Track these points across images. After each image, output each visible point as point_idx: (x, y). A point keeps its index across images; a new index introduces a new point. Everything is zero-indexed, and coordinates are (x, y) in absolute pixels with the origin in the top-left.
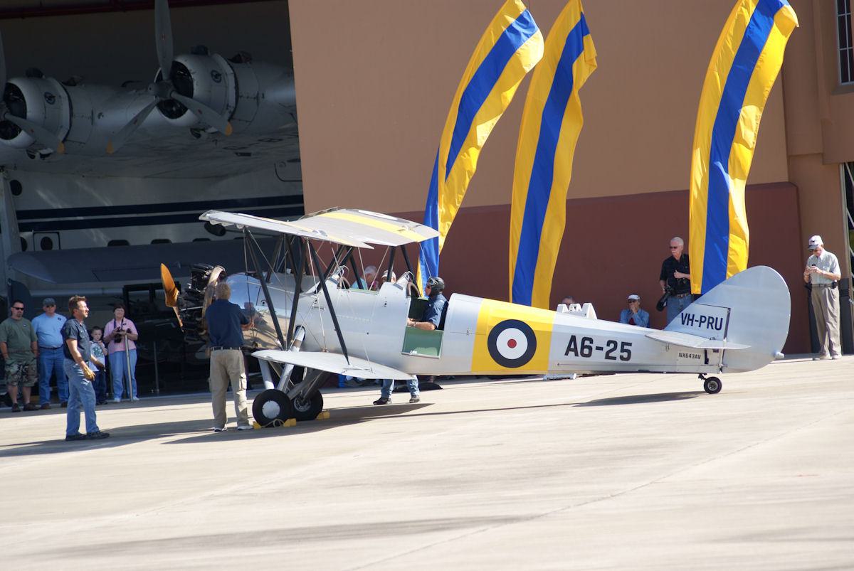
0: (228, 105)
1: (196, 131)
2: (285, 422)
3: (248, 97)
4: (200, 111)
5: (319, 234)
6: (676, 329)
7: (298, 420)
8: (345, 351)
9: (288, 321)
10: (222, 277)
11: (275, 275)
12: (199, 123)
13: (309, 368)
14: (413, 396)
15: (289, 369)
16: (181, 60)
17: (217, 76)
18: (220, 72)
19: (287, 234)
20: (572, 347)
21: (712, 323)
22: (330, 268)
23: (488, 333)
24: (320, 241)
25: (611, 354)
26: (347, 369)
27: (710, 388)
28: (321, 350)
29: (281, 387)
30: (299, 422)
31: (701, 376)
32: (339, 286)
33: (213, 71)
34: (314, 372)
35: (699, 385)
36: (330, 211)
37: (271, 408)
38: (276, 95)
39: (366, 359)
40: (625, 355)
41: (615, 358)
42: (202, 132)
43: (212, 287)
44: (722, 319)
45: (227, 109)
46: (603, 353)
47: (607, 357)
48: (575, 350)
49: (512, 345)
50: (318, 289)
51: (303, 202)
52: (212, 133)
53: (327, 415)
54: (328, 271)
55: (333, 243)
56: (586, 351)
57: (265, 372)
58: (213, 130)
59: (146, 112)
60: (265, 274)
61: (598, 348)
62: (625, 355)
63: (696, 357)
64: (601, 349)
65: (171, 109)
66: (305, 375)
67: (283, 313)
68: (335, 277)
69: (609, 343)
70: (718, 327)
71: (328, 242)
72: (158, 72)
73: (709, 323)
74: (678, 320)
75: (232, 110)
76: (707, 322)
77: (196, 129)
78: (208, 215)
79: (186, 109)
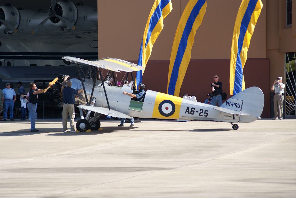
0: (74, 20)
1: (62, 28)
2: (87, 130)
3: (81, 18)
4: (64, 22)
5: (103, 66)
6: (224, 107)
7: (91, 130)
8: (109, 107)
9: (90, 96)
10: (68, 79)
11: (87, 80)
12: (64, 25)
13: (96, 113)
14: (132, 124)
15: (90, 112)
16: (59, 3)
17: (71, 10)
18: (72, 8)
19: (92, 66)
20: (188, 111)
21: (236, 105)
22: (106, 78)
23: (159, 104)
24: (103, 69)
25: (201, 114)
26: (109, 114)
27: (234, 128)
28: (101, 106)
29: (86, 118)
30: (92, 131)
31: (232, 124)
32: (108, 85)
33: (70, 8)
34: (98, 114)
35: (231, 127)
36: (107, 58)
37: (82, 125)
38: (91, 17)
39: (116, 110)
40: (206, 114)
41: (202, 115)
42: (64, 29)
43: (65, 82)
44: (240, 104)
45: (74, 21)
46: (198, 114)
47: (200, 115)
48: (189, 112)
49: (167, 109)
50: (101, 85)
51: (98, 55)
52: (68, 29)
53: (101, 129)
54: (105, 79)
55: (107, 70)
56: (192, 113)
57: (81, 113)
58: (68, 28)
59: (46, 20)
60: (83, 79)
61: (196, 112)
62: (206, 114)
63: (230, 117)
64: (197, 112)
65: (55, 20)
66: (95, 114)
67: (89, 93)
68: (107, 81)
69: (200, 110)
70: (239, 107)
71: (106, 69)
72: (51, 7)
73: (235, 105)
74: (225, 103)
75: (75, 22)
76: (235, 105)
77: (62, 27)
78: (65, 57)
79: (60, 21)
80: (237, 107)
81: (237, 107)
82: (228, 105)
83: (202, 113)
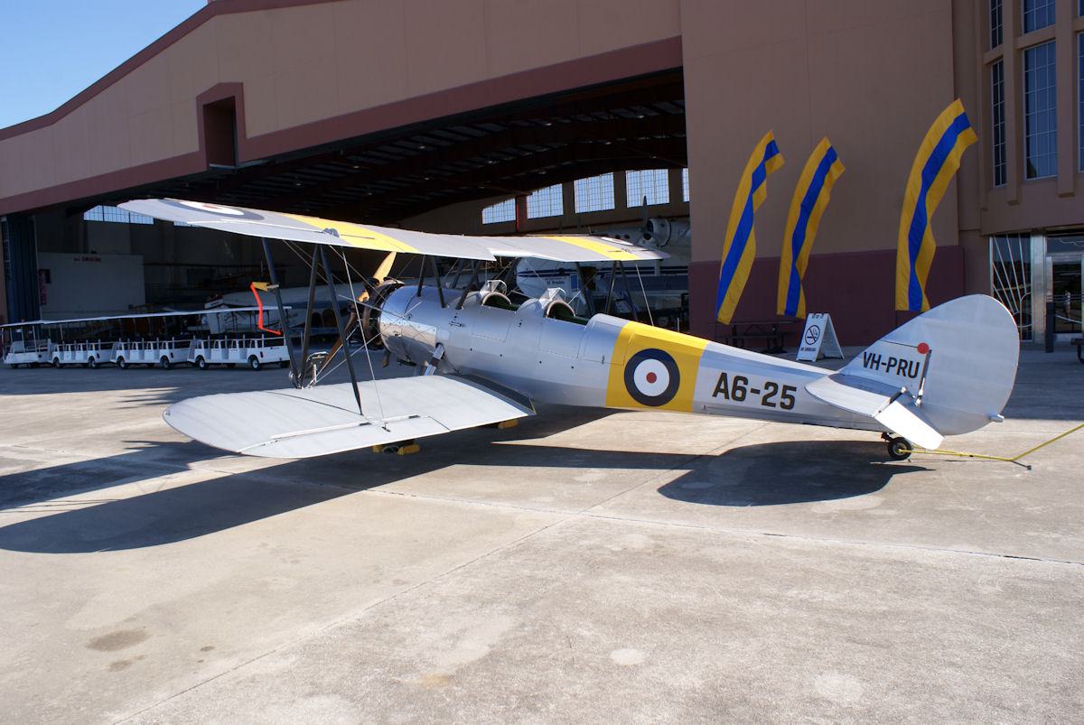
20: (722, 387)
25: (769, 400)
40: (787, 402)
41: (774, 405)
44: (918, 364)
47: (765, 402)
48: (725, 390)
56: (739, 394)
61: (753, 391)
62: (787, 402)
64: (756, 391)
69: (768, 385)
70: (913, 374)
73: (900, 368)
74: (859, 361)
76: (897, 365)
80: (904, 375)
81: (904, 375)
82: (871, 367)
83: (774, 397)
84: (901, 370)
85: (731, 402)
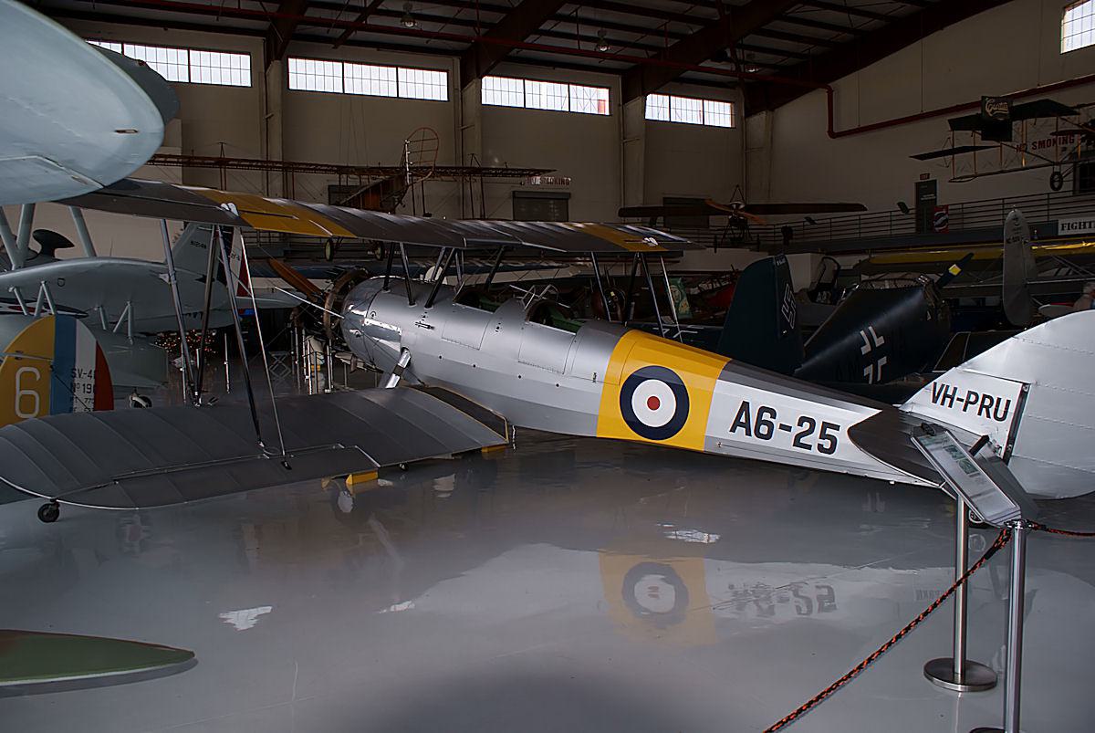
20: (743, 420)
21: (987, 405)
25: (803, 440)
40: (827, 444)
41: (809, 447)
44: (1008, 402)
47: (797, 443)
48: (747, 425)
56: (764, 430)
61: (782, 427)
62: (827, 444)
64: (789, 429)
69: (802, 421)
70: (1000, 415)
73: (982, 406)
76: (979, 402)
80: (988, 416)
81: (988, 416)
82: (943, 404)
84: (984, 409)
85: (753, 439)
